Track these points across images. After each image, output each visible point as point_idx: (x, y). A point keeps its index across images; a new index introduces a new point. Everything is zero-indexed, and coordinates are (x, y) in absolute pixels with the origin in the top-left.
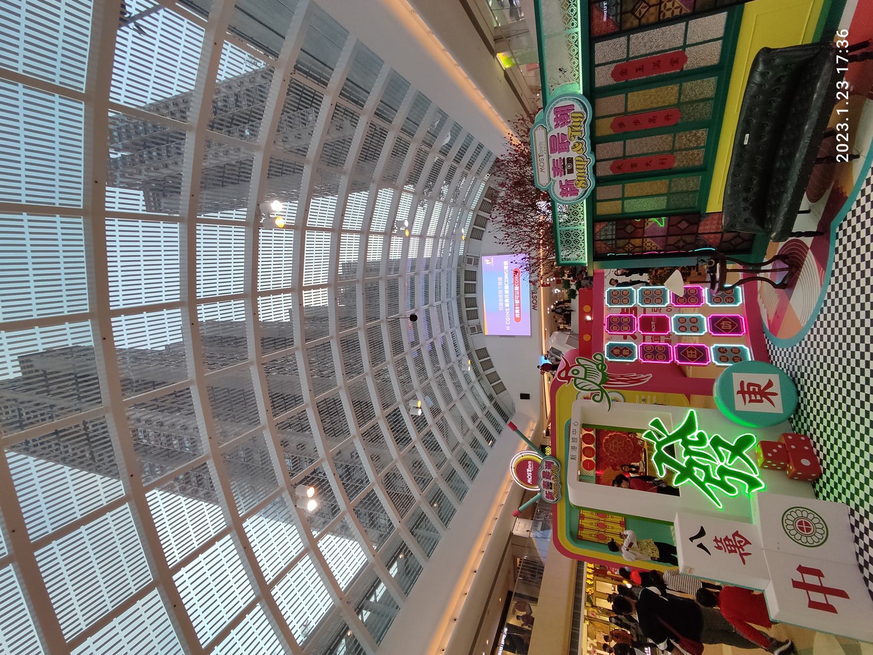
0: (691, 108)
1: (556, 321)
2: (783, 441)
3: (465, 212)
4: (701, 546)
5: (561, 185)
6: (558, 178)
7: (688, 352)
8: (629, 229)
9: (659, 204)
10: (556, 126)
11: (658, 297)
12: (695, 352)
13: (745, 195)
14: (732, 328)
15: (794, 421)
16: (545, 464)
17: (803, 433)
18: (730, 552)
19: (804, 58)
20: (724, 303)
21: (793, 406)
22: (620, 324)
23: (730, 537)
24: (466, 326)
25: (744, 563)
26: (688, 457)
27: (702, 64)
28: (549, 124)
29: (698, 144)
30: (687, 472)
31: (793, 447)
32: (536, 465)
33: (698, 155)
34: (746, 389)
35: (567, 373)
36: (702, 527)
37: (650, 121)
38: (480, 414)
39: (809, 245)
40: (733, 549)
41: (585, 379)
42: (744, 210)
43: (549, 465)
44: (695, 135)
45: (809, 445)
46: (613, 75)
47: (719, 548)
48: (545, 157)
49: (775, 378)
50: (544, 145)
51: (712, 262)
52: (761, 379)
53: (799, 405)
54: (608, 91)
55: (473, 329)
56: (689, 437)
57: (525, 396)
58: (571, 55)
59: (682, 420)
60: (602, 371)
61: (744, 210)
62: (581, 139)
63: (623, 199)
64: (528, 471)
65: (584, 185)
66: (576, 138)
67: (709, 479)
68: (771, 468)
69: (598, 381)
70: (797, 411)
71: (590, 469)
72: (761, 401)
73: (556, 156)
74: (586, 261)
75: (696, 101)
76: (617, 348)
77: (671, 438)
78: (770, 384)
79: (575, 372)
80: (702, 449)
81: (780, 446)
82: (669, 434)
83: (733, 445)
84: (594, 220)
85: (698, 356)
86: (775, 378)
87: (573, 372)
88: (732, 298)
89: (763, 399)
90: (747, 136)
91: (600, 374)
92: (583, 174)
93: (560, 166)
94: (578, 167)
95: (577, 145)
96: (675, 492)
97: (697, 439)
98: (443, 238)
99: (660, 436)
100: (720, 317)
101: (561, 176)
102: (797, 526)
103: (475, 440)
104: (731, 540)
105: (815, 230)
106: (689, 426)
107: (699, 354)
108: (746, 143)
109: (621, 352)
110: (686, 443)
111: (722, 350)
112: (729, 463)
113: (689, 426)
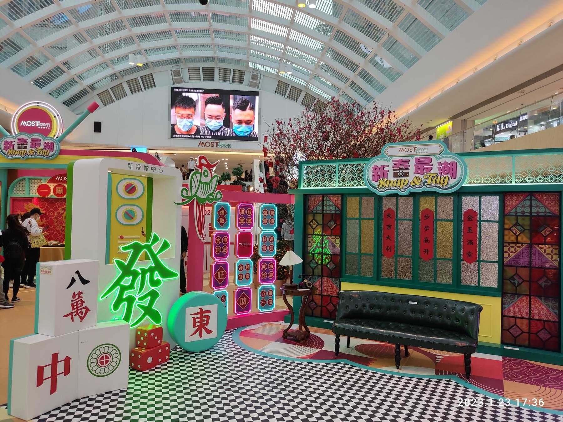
0: (430, 268)
1: (183, 166)
2: (162, 344)
3: (307, 78)
4: (73, 280)
5: (384, 167)
6: (391, 164)
7: (222, 272)
8: (332, 224)
9: (352, 247)
10: (440, 164)
11: (268, 248)
12: (222, 278)
13: (368, 305)
14: (241, 305)
15: (175, 352)
16: (50, 141)
17: (170, 358)
18: (72, 305)
19: (471, 333)
20: (261, 298)
21: (190, 349)
22: (246, 216)
23: (84, 305)
24: (181, 65)
25: (64, 316)
26: (140, 272)
27: (463, 274)
28: (443, 157)
29: (399, 274)
30: (127, 271)
31: (160, 351)
32: (46, 132)
33: (390, 274)
34: (204, 315)
35: (204, 165)
36: (89, 282)
37: (426, 238)
38: (74, 72)
39: (323, 349)
40: (75, 307)
41: (200, 182)
42: (356, 305)
43: (50, 146)
44: (407, 271)
45: (162, 362)
46: (470, 210)
47: (74, 296)
48: (413, 153)
49: (214, 335)
50: (424, 152)
51: (310, 286)
52: (213, 325)
53: (193, 353)
54: (458, 206)
55: (177, 73)
56: (156, 273)
57: (97, 127)
58: (495, 177)
59: (169, 266)
60: (208, 198)
61: (356, 305)
62: (424, 184)
63: (360, 219)
64: (38, 122)
65: (381, 186)
66: (425, 180)
67: (123, 289)
68: (137, 337)
69: (199, 194)
70: (187, 352)
71: (39, 192)
72: (194, 326)
73: (412, 163)
74: (302, 188)
75: (436, 271)
76: (225, 213)
77: (154, 257)
78: (209, 332)
79: (206, 174)
80: (147, 283)
81: (159, 341)
82: (158, 256)
83: (153, 308)
84: (343, 195)
85: (219, 280)
86: (214, 335)
87: (206, 171)
88: (264, 304)
89: (197, 328)
90: (416, 303)
91: (205, 197)
92: (391, 185)
93: (403, 166)
94: (399, 181)
95: (419, 181)
96: (108, 261)
97: (155, 279)
98: (285, 49)
99: (155, 247)
100: (250, 297)
101: (393, 167)
102: (104, 355)
103: (38, 64)
104: (82, 305)
105: (340, 351)
106: (166, 273)
107: (220, 280)
108: (410, 302)
109: (222, 216)
110: (151, 270)
111: (224, 298)
112: (138, 305)
113: (166, 273)
